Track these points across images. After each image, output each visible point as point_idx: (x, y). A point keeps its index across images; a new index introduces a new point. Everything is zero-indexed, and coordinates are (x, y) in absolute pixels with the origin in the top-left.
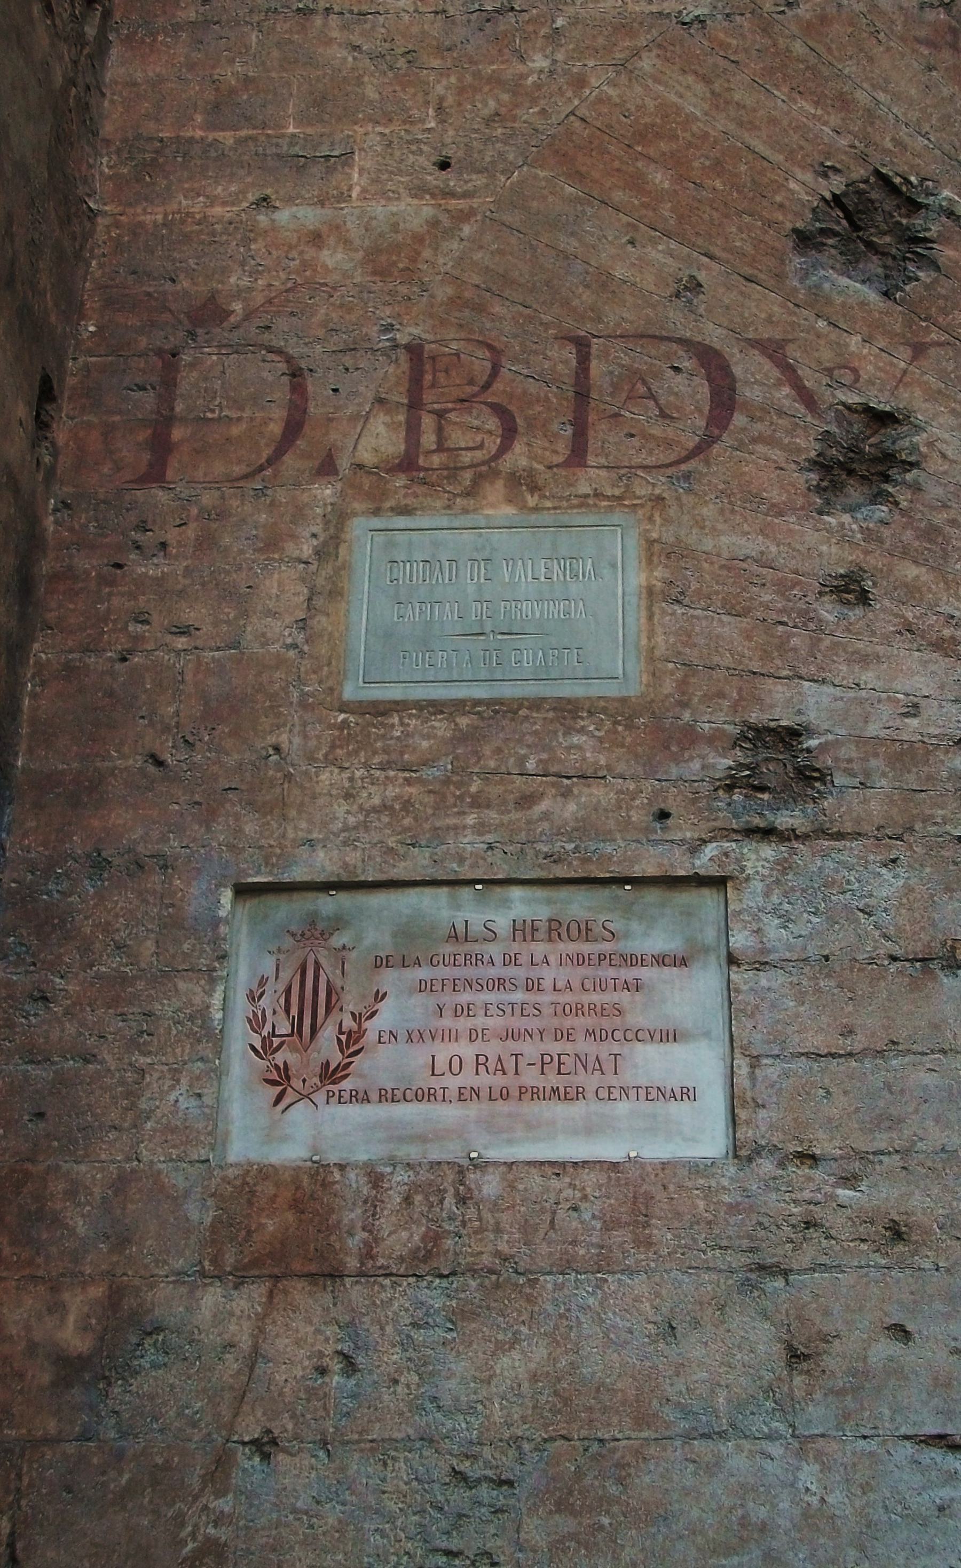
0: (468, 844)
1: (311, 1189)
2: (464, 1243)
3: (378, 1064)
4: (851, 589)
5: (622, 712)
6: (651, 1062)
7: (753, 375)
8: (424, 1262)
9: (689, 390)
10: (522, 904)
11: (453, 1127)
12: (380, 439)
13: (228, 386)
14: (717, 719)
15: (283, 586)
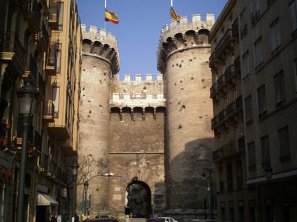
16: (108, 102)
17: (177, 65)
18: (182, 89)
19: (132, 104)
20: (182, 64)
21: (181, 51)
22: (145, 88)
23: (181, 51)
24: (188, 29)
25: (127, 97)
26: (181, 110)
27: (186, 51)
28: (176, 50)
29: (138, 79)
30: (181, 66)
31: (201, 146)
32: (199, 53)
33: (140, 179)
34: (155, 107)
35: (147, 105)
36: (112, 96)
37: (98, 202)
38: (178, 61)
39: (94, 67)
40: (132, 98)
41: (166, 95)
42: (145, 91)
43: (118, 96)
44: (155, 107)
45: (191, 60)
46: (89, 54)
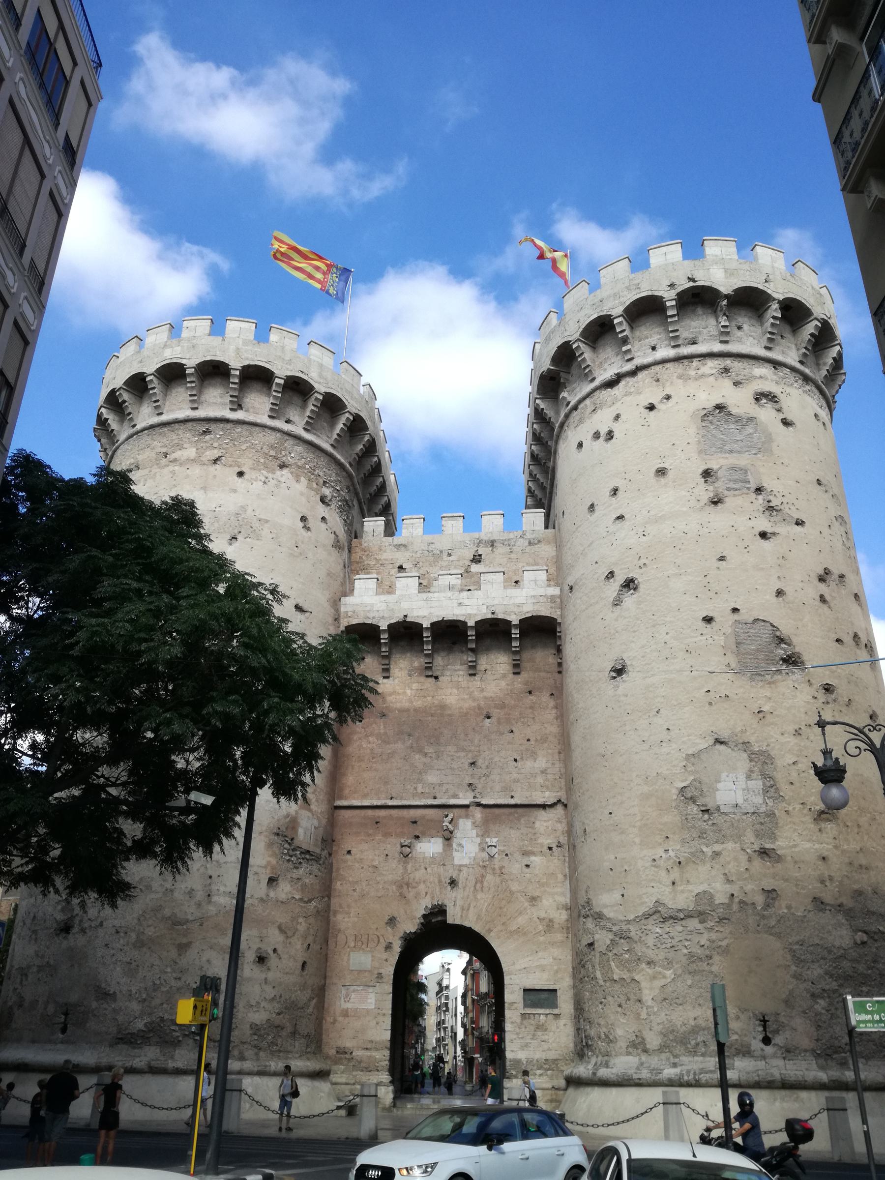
0: (358, 983)
1: (347, 1010)
2: (357, 1014)
3: (351, 1000)
4: (386, 960)
5: (369, 971)
6: (369, 1001)
7: (381, 938)
8: (354, 1016)
9: (376, 940)
10: (362, 988)
11: (357, 1006)
12: (352, 944)
13: (341, 938)
14: (376, 972)
15: (345, 958)
16: (335, 603)
17: (597, 436)
18: (621, 517)
19: (426, 610)
20: (617, 428)
21: (611, 384)
22: (477, 559)
23: (611, 384)
24: (631, 297)
25: (407, 585)
26: (617, 602)
27: (630, 380)
28: (588, 388)
29: (453, 528)
30: (610, 435)
31: (718, 741)
32: (680, 377)
33: (454, 917)
34: (515, 620)
35: (484, 613)
36: (352, 583)
37: (259, 1017)
38: (602, 421)
39: (282, 466)
40: (423, 587)
41: (558, 572)
42: (475, 568)
43: (372, 584)
44: (515, 620)
45: (651, 408)
46: (265, 420)
